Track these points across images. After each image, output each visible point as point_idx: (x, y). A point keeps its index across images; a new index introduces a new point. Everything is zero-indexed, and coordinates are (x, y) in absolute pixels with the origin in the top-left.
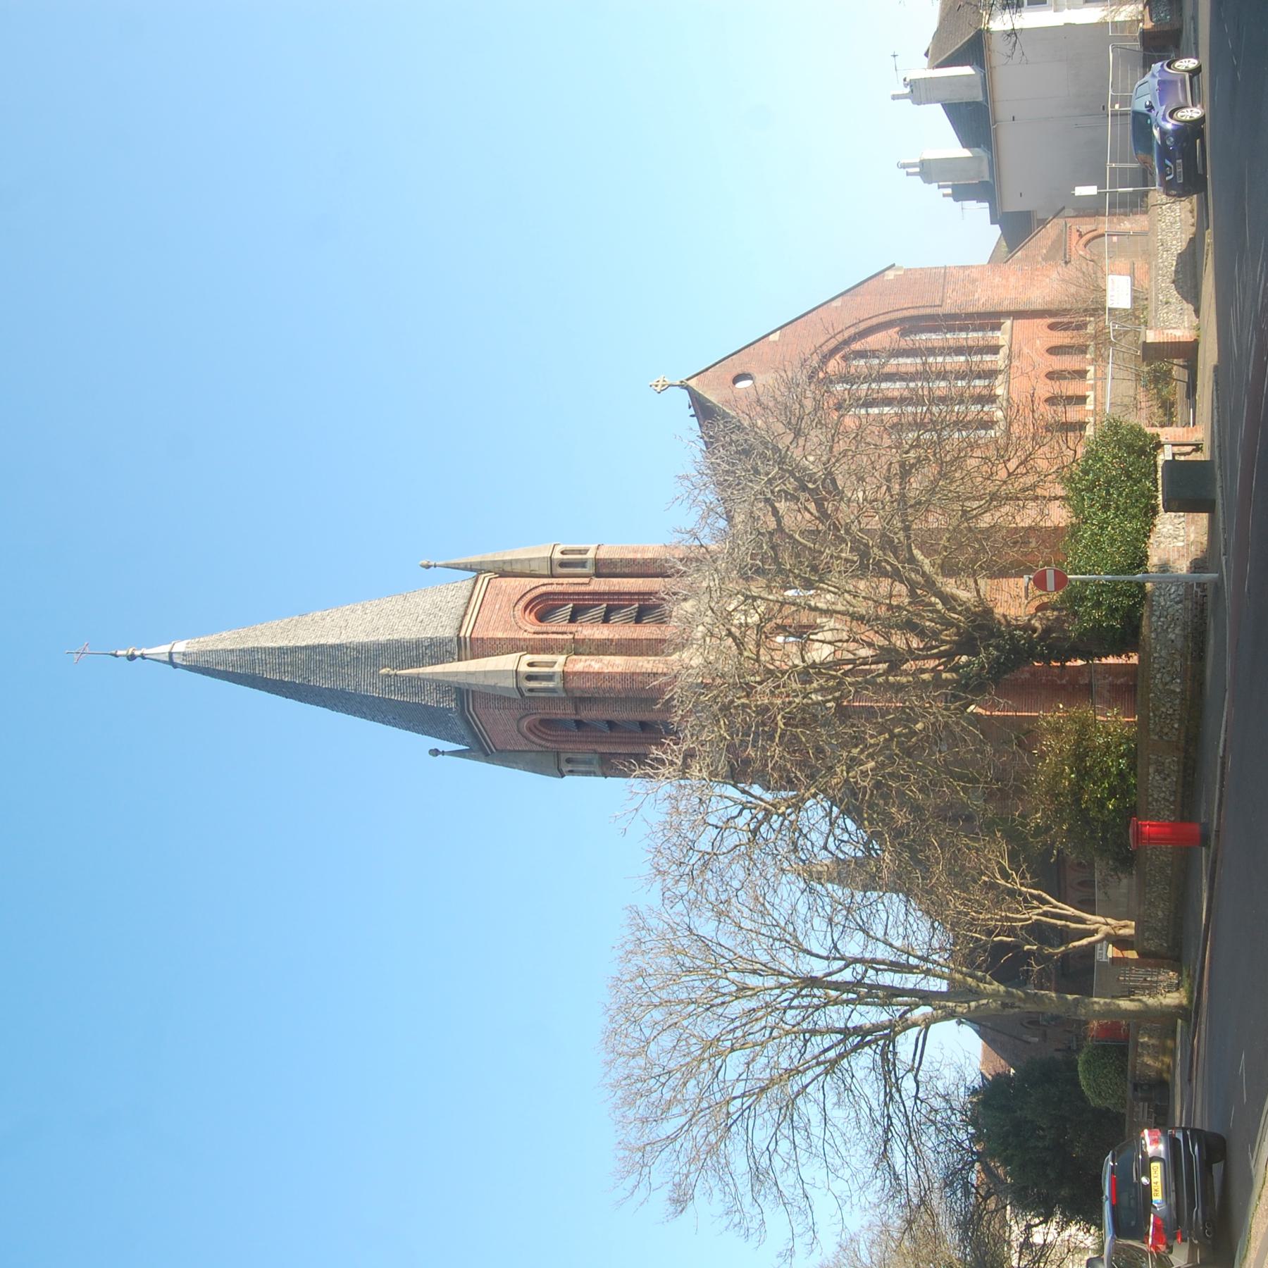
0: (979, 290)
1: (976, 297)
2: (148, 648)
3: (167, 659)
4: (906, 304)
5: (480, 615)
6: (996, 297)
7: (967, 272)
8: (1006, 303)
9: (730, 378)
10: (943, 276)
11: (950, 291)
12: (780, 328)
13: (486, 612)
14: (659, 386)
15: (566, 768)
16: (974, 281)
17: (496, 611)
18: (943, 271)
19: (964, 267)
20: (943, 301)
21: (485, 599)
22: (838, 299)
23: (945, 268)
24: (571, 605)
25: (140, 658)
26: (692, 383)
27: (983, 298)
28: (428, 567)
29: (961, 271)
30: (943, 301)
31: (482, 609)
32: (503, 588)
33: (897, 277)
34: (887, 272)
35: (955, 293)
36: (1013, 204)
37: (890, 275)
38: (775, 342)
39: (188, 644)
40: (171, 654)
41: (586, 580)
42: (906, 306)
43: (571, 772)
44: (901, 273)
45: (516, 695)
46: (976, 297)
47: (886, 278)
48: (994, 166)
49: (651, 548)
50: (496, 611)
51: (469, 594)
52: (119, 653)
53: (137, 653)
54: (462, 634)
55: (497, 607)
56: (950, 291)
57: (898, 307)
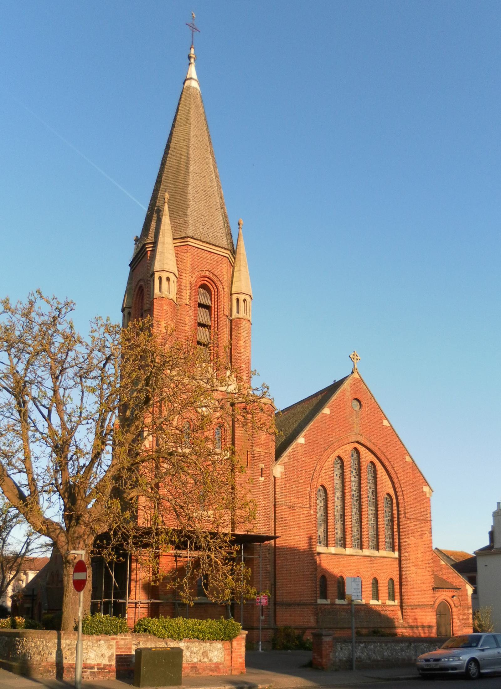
0: (415, 539)
1: (411, 538)
2: (196, 67)
3: (188, 77)
4: (407, 498)
5: (203, 251)
6: (410, 549)
10: (426, 520)
11: (414, 523)
13: (205, 254)
17: (205, 260)
21: (214, 254)
23: (431, 520)
27: (410, 541)
31: (207, 252)
35: (413, 525)
39: (196, 89)
40: (191, 79)
46: (411, 538)
50: (205, 260)
51: (217, 244)
52: (192, 50)
53: (192, 60)
56: (414, 523)
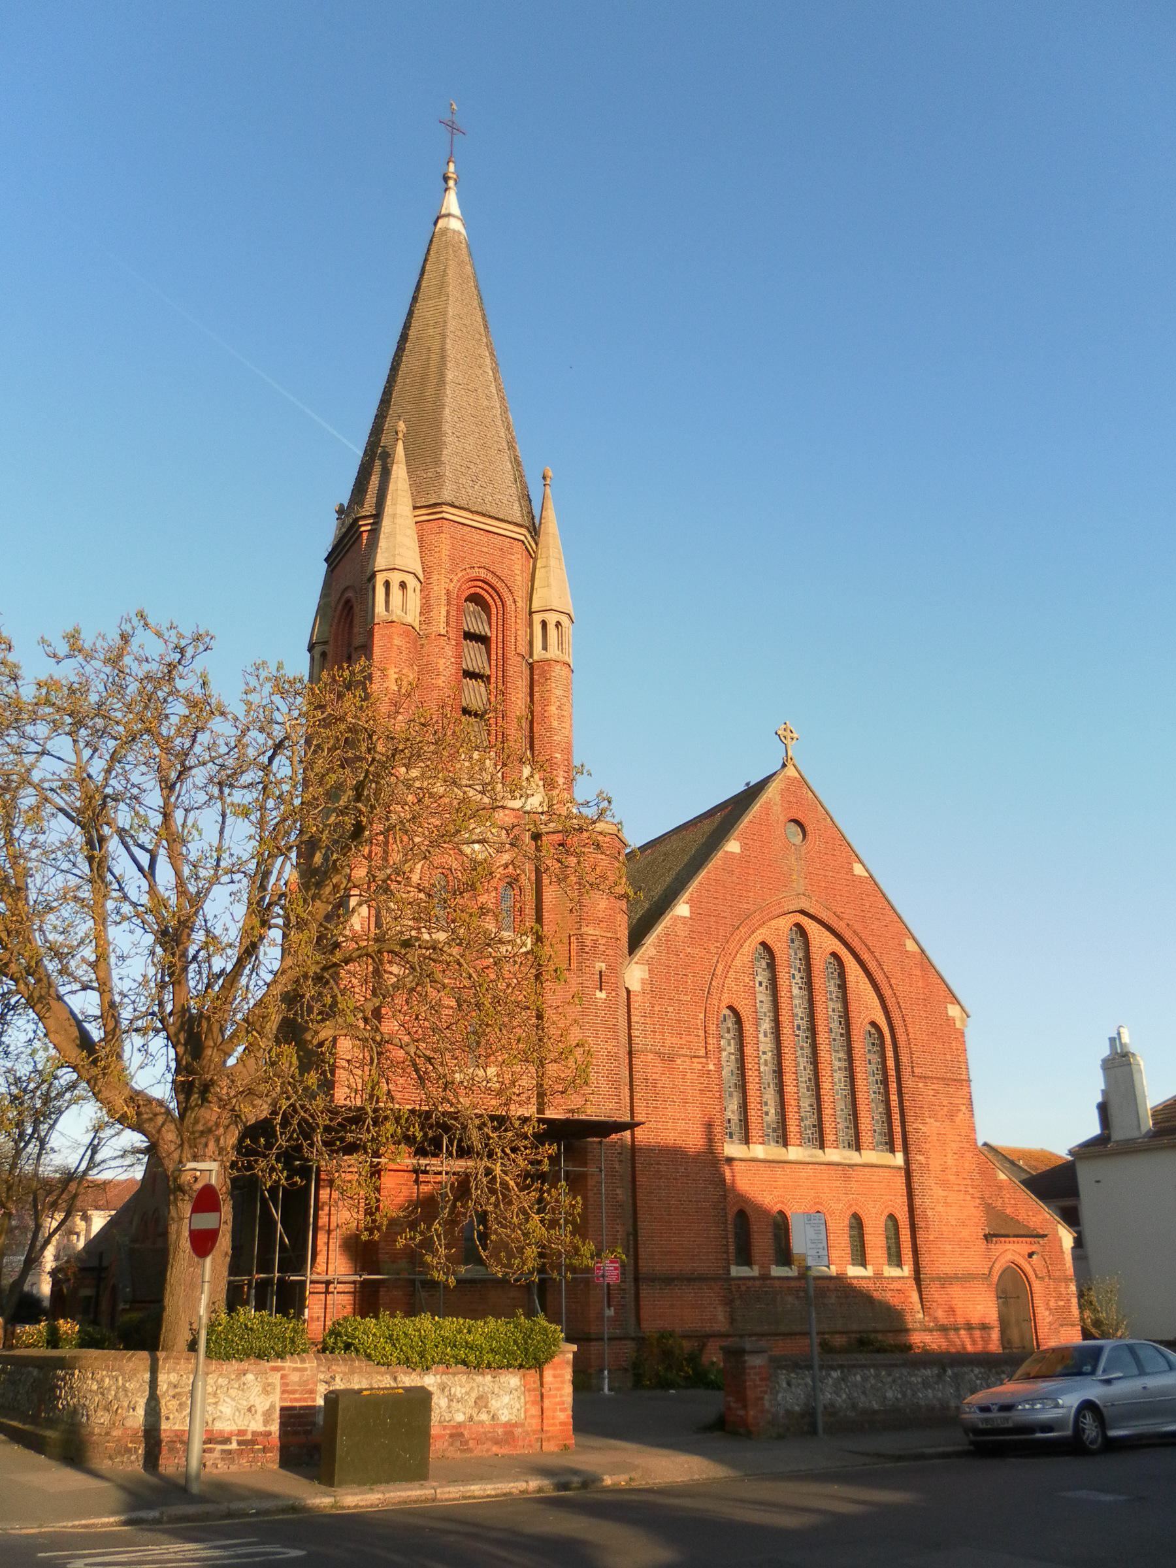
0: (938, 1124)
3: (443, 212)
6: (928, 1146)
7: (963, 1108)
8: (920, 1158)
9: (799, 817)
12: (871, 876)
14: (785, 734)
15: (318, 650)
16: (951, 1116)
17: (478, 548)
18: (963, 1077)
19: (970, 1104)
20: (920, 1077)
22: (916, 947)
23: (969, 1080)
24: (489, 634)
25: (445, 186)
26: (791, 772)
27: (927, 1127)
28: (544, 478)
29: (965, 1101)
30: (920, 1077)
32: (509, 556)
33: (950, 1021)
34: (958, 1007)
35: (931, 1092)
36: (1085, 1176)
37: (953, 1011)
38: (852, 869)
39: (459, 233)
40: (448, 215)
41: (522, 649)
42: (911, 1030)
43: (312, 659)
44: (958, 1025)
45: (368, 574)
47: (949, 1006)
48: (1130, 1148)
49: (563, 725)
50: (478, 548)
53: (451, 183)
54: (445, 508)
55: (485, 549)
57: (909, 1020)
